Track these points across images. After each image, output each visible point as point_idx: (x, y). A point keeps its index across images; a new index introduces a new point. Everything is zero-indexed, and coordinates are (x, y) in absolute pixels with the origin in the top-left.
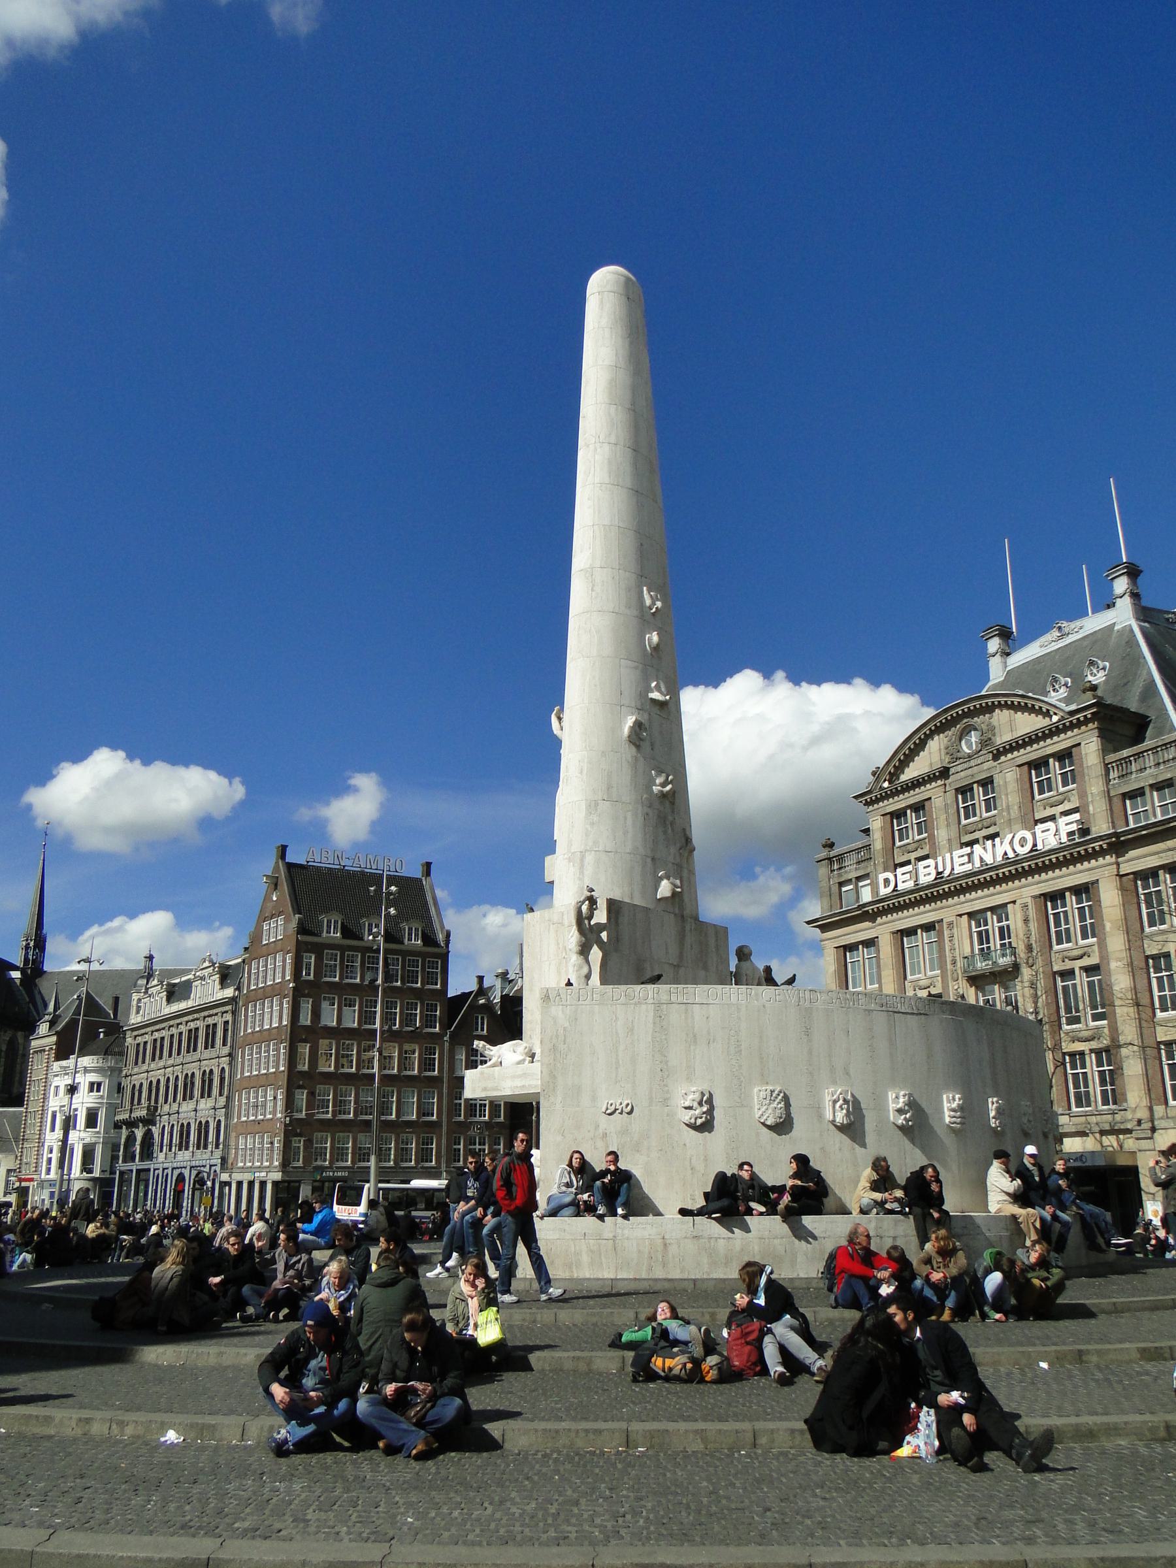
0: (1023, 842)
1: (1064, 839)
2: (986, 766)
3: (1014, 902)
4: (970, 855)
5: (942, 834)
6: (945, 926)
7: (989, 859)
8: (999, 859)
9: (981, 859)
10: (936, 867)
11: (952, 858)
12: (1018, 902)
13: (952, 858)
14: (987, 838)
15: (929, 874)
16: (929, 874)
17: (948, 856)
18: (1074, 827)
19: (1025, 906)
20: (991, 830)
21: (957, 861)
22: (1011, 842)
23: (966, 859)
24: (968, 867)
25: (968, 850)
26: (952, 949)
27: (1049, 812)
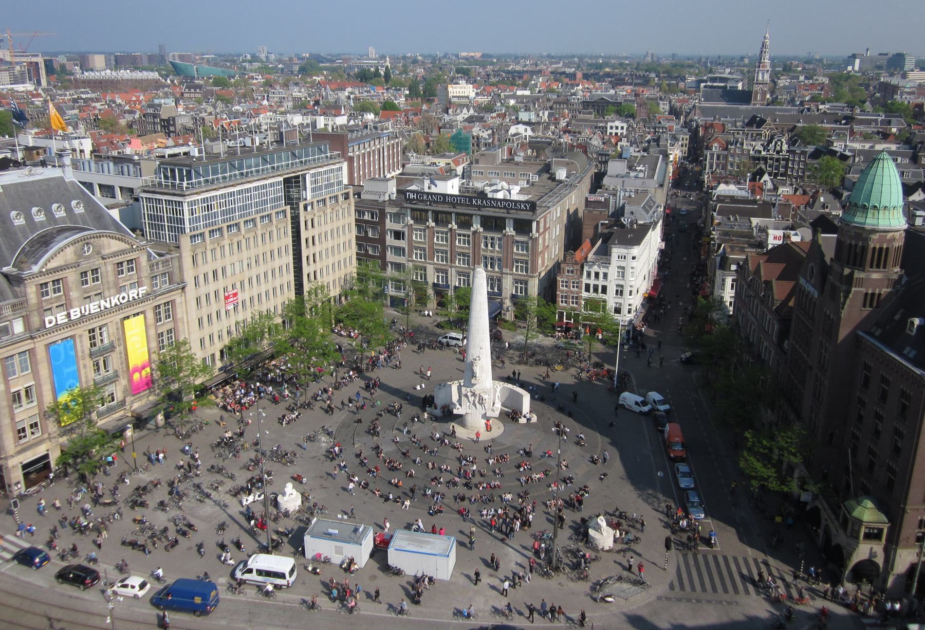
0: (123, 298)
1: (140, 296)
2: (97, 263)
5: (74, 294)
6: (77, 337)
7: (108, 306)
8: (113, 305)
10: (81, 312)
17: (87, 306)
19: (117, 323)
20: (99, 291)
21: (92, 308)
22: (118, 299)
23: (97, 307)
24: (99, 310)
26: (82, 346)
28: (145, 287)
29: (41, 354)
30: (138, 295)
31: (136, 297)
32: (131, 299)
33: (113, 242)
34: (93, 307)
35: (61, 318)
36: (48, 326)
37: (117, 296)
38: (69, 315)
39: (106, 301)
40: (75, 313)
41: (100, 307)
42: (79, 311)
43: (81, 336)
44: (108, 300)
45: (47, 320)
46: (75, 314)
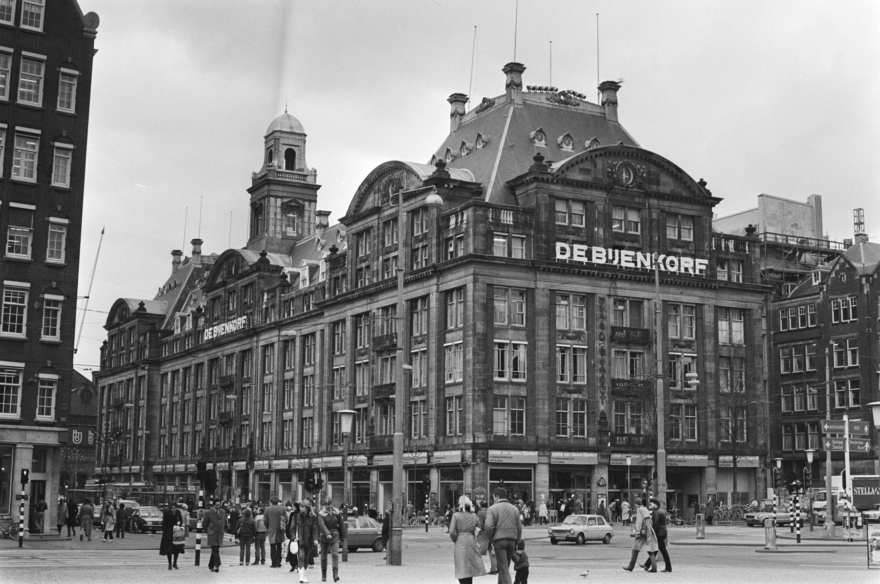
0: (672, 263)
1: (697, 272)
3: (649, 300)
4: (635, 257)
6: (597, 300)
9: (642, 264)
10: (607, 256)
11: (620, 254)
12: (654, 301)
13: (620, 254)
14: (630, 249)
15: (601, 258)
16: (601, 258)
17: (617, 251)
18: (704, 267)
20: (636, 245)
21: (623, 258)
24: (632, 265)
25: (632, 253)
27: (675, 250)
28: (706, 262)
29: (542, 301)
30: (694, 268)
31: (691, 271)
32: (683, 271)
33: (664, 178)
34: (625, 259)
35: (578, 254)
36: (559, 256)
37: (662, 256)
38: (589, 254)
39: (645, 258)
40: (599, 255)
41: (636, 263)
42: (604, 253)
43: (602, 300)
44: (648, 255)
45: (559, 245)
46: (600, 255)
